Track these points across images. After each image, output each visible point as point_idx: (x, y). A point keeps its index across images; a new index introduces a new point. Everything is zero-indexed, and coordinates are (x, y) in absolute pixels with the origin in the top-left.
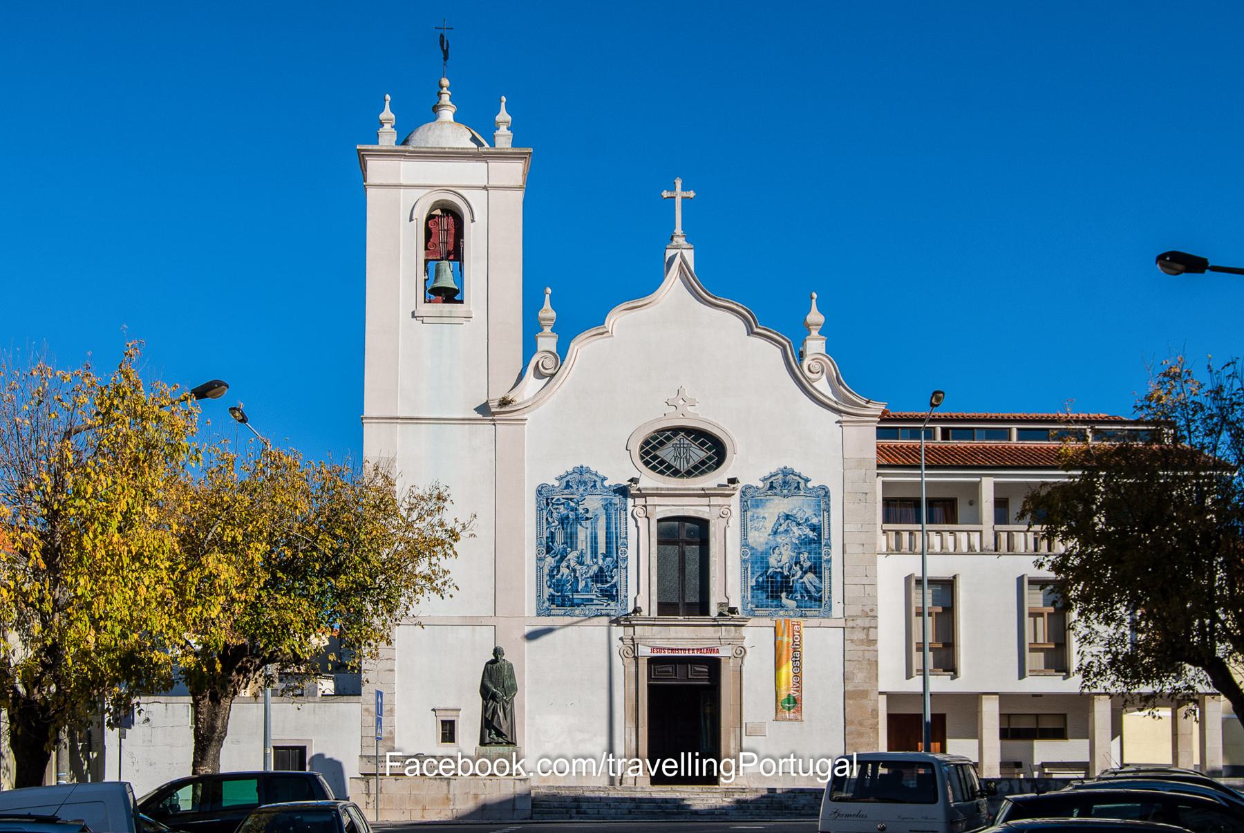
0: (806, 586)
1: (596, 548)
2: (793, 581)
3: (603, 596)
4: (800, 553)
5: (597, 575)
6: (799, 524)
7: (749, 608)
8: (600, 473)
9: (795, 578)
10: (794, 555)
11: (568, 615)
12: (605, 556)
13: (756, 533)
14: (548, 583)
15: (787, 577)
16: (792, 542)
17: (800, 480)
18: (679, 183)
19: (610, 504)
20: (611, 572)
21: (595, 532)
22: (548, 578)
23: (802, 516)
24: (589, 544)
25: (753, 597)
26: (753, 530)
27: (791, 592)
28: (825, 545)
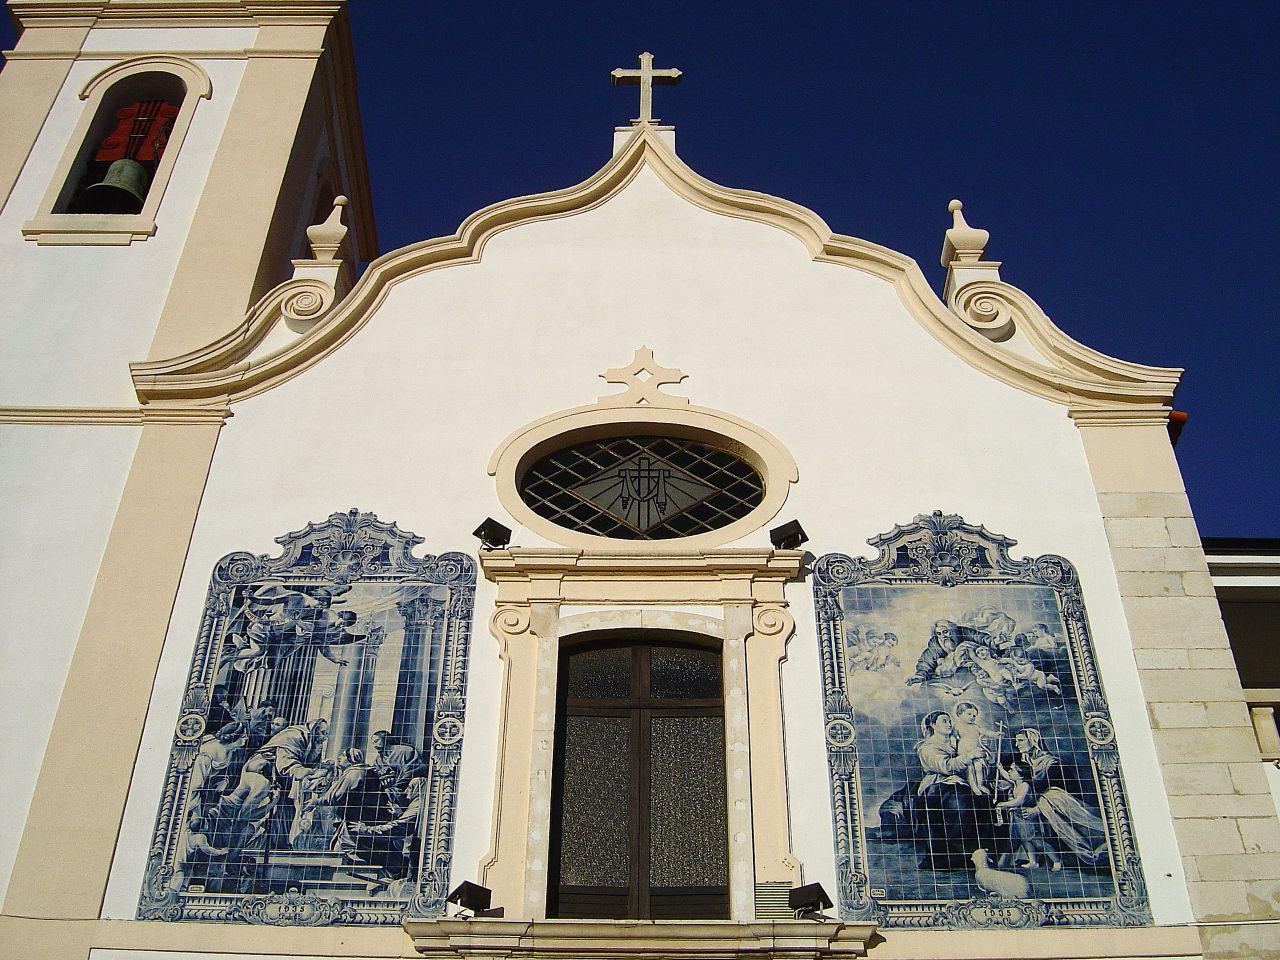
0: (1048, 827)
1: (364, 717)
2: (1004, 812)
3: (367, 858)
4: (1014, 732)
5: (354, 796)
6: (1001, 653)
7: (866, 899)
8: (402, 527)
9: (1011, 803)
10: (998, 735)
11: (242, 919)
12: (389, 741)
13: (872, 677)
14: (195, 817)
15: (983, 801)
16: (984, 701)
17: (984, 543)
18: (646, 59)
19: (422, 601)
20: (404, 786)
21: (365, 673)
22: (197, 802)
23: (1004, 629)
24: (343, 707)
25: (876, 863)
26: (860, 671)
27: (1003, 846)
28: (1089, 708)
